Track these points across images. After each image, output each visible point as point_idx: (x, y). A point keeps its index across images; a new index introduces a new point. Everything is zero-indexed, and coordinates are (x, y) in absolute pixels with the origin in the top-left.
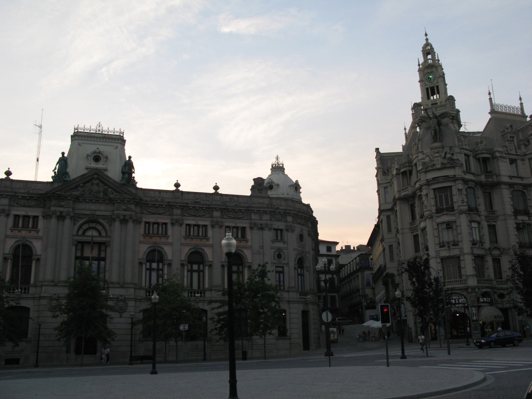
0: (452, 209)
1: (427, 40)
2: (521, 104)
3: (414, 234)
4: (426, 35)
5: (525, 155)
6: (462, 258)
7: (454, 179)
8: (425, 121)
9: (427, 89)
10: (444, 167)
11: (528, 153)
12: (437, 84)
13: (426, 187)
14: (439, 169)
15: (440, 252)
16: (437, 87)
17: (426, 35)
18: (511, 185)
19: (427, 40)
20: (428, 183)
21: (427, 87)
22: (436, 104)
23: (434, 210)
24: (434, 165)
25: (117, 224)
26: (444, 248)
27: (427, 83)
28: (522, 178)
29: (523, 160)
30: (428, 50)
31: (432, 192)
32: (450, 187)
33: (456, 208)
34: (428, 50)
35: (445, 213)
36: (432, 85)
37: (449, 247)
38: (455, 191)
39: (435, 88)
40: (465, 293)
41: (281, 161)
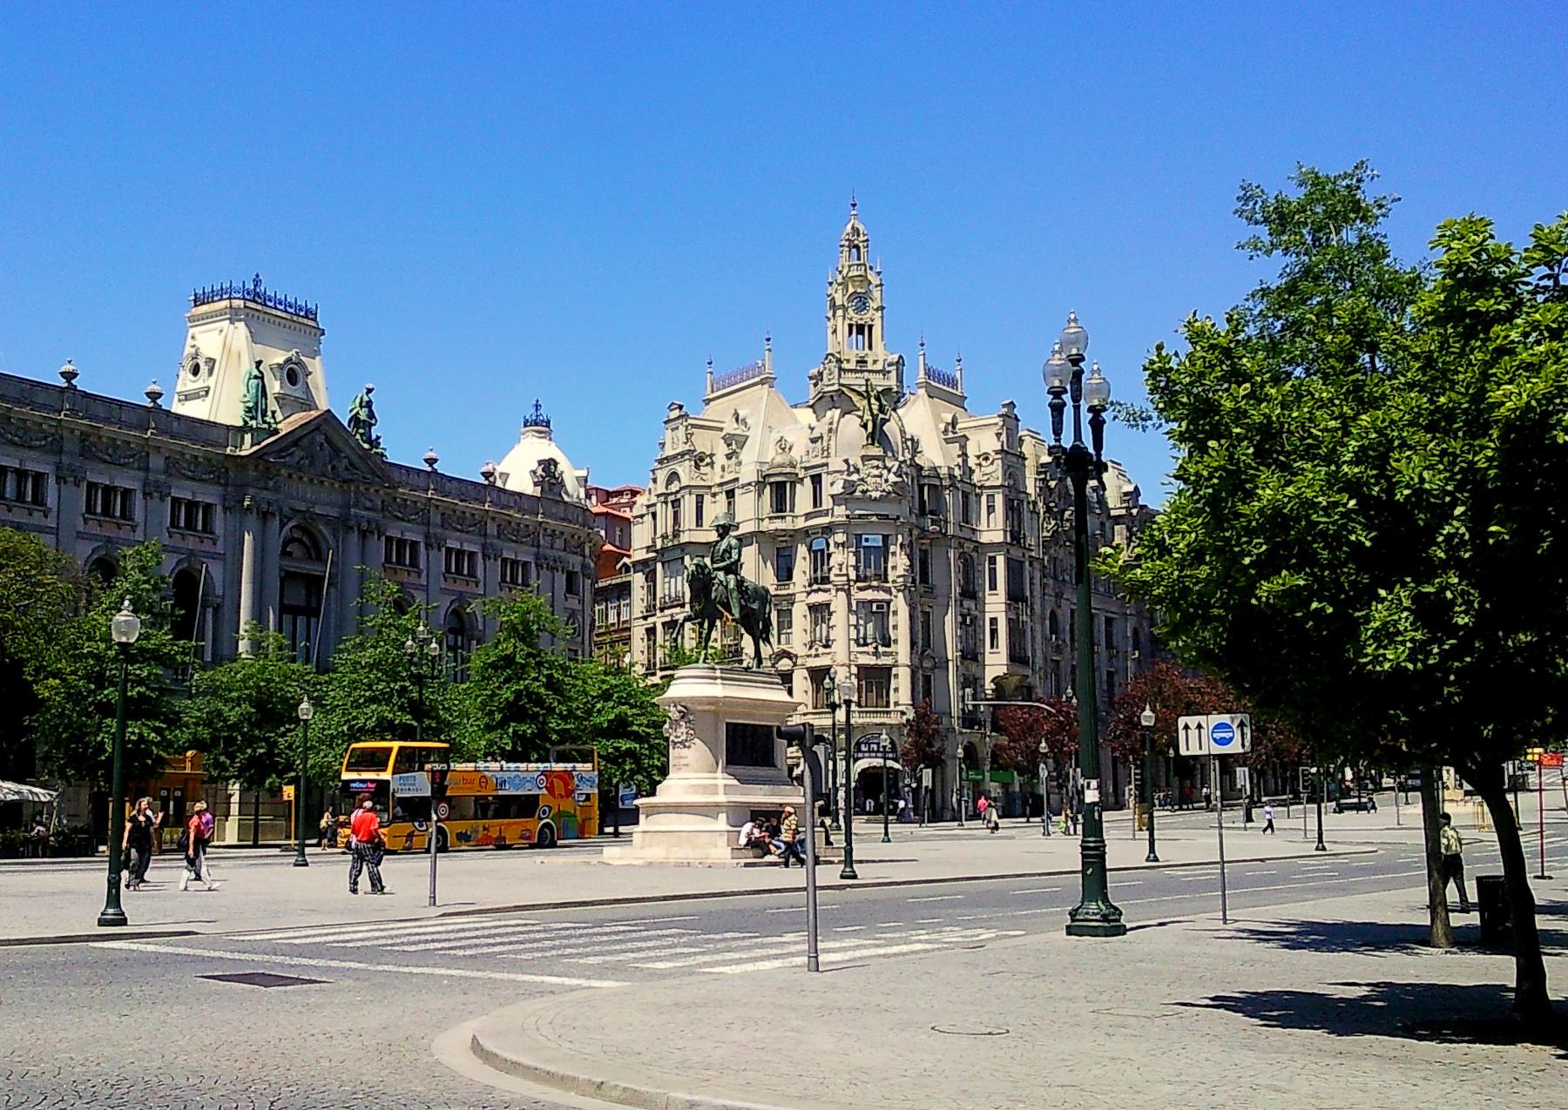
9: (850, 326)
11: (987, 484)
16: (870, 327)
23: (853, 576)
25: (354, 537)
41: (544, 413)
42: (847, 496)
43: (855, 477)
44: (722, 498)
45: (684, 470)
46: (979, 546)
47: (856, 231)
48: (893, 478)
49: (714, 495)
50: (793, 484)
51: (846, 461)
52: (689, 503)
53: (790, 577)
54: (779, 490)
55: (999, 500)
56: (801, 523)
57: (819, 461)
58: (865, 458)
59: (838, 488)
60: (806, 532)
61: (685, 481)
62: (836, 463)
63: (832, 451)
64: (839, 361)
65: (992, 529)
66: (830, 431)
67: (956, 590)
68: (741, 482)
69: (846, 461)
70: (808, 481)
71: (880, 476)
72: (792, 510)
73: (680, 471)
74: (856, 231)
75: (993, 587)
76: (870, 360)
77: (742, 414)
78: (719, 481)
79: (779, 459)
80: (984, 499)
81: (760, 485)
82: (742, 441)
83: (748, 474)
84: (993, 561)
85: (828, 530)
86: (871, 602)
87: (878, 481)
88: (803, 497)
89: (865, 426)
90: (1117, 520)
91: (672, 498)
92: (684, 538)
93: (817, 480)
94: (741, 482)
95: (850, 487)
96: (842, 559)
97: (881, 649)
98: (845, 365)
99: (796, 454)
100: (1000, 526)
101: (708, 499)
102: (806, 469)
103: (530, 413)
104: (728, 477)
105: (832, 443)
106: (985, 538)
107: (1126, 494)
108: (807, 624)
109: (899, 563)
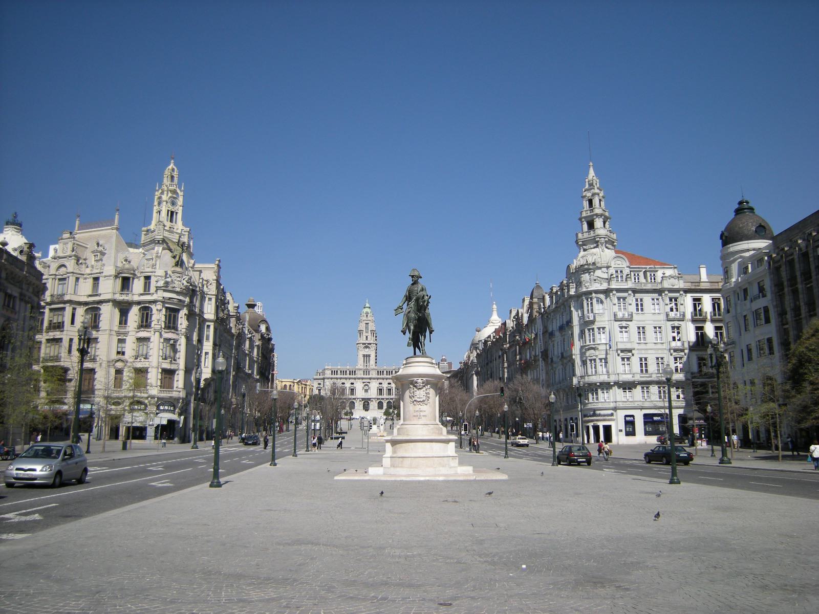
3: (120, 337)
9: (168, 211)
11: (209, 293)
15: (163, 363)
16: (177, 213)
20: (164, 301)
21: (169, 209)
23: (163, 326)
26: (166, 361)
35: (173, 331)
36: (174, 210)
39: (175, 213)
41: (19, 219)
42: (166, 287)
43: (169, 280)
44: (91, 281)
45: (71, 265)
46: (205, 320)
47: (173, 170)
48: (186, 284)
49: (85, 279)
50: (133, 279)
51: (166, 272)
52: (72, 280)
53: (126, 323)
54: (126, 283)
55: (214, 300)
56: (136, 298)
58: (173, 272)
59: (161, 283)
60: (139, 303)
61: (70, 269)
62: (160, 272)
63: (157, 266)
64: (164, 226)
65: (209, 311)
68: (103, 274)
69: (166, 272)
70: (142, 279)
72: (132, 291)
73: (67, 264)
74: (173, 170)
76: (175, 227)
77: (101, 243)
78: (88, 271)
79: (127, 266)
80: (207, 299)
81: (116, 277)
82: (103, 254)
83: (110, 270)
84: (208, 326)
85: (155, 302)
86: (170, 339)
87: (179, 283)
88: (138, 285)
90: (233, 316)
91: (60, 277)
92: (67, 298)
93: (148, 278)
94: (103, 274)
95: (167, 283)
96: (158, 316)
97: (173, 362)
98: (166, 228)
99: (134, 264)
100: (213, 311)
101: (81, 280)
102: (142, 272)
103: (11, 218)
104: (95, 271)
106: (206, 316)
107: (235, 307)
108: (134, 346)
109: (183, 322)
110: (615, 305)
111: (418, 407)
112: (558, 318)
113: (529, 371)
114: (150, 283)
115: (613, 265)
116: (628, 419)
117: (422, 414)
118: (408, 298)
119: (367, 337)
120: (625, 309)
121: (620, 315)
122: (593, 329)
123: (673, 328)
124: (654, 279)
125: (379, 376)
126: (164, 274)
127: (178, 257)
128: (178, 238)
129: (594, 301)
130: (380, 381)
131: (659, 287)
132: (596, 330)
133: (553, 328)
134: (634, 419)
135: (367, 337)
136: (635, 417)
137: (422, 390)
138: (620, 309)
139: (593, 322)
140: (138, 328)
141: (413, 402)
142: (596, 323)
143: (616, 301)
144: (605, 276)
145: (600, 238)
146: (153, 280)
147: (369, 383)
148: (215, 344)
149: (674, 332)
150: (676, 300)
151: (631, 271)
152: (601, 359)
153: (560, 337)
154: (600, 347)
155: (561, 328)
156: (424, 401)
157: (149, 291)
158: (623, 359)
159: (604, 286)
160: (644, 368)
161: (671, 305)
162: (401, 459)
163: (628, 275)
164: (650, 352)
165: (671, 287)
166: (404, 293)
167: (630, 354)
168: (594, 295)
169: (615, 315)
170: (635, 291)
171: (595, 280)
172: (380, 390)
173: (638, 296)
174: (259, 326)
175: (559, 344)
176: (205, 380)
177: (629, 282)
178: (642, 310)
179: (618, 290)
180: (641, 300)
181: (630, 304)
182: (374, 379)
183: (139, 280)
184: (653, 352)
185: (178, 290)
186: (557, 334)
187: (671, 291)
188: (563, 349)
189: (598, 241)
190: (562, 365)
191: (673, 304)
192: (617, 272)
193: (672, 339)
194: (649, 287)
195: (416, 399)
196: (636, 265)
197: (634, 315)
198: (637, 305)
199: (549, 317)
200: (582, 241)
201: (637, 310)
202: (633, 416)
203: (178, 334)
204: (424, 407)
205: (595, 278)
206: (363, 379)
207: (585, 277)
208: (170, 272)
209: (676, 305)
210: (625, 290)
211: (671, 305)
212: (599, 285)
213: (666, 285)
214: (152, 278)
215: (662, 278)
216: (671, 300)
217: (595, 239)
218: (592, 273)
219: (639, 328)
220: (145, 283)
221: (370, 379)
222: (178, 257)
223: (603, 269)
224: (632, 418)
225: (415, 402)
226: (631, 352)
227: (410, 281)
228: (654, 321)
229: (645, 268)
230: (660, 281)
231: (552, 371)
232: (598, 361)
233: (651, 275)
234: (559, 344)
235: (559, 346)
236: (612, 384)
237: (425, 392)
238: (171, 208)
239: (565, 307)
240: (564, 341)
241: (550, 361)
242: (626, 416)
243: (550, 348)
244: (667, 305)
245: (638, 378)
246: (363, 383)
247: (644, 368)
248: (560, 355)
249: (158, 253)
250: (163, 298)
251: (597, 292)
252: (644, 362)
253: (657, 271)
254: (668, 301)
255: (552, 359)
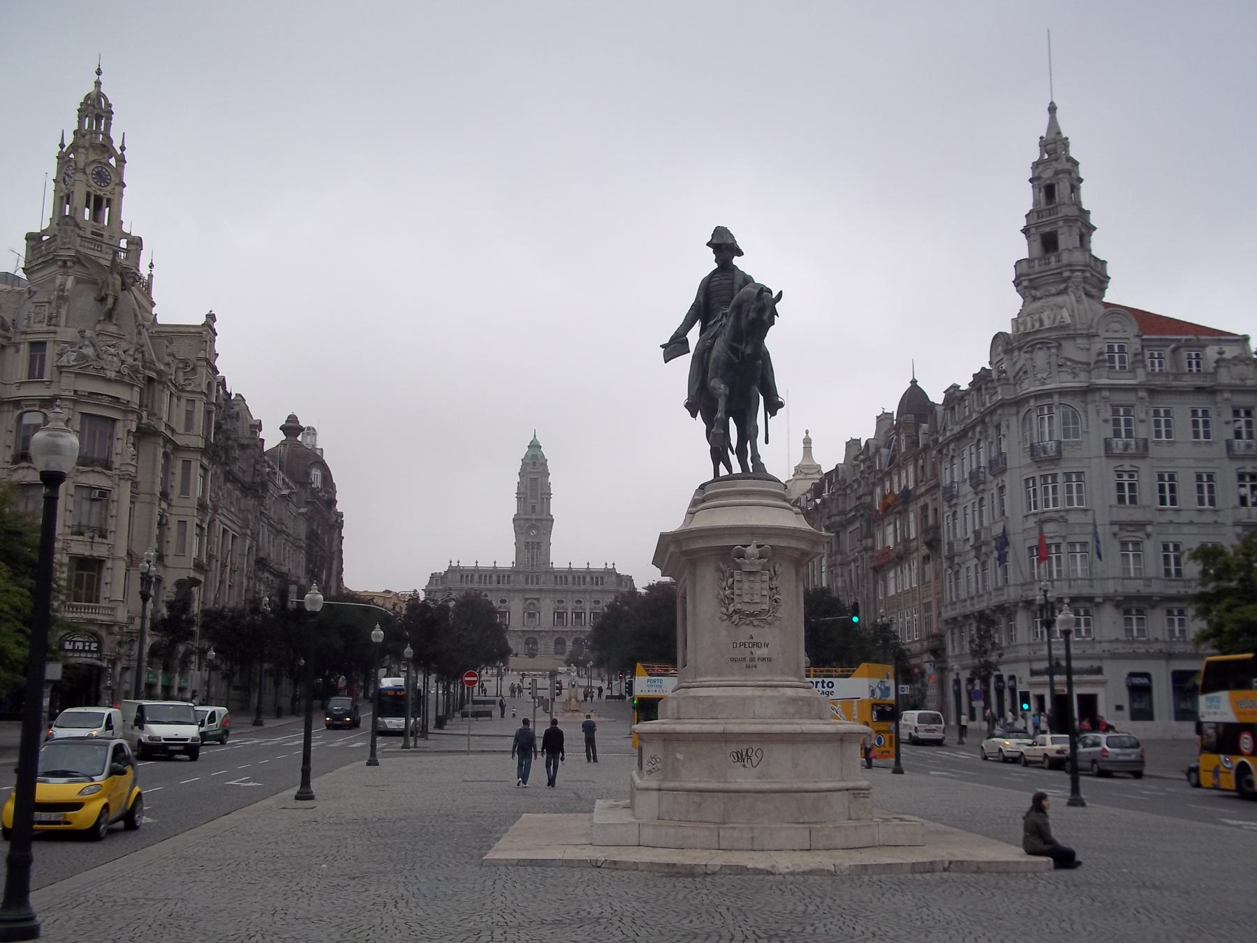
0: (107, 465)
1: (98, 84)
2: (151, 276)
4: (99, 72)
5: (183, 390)
6: (109, 564)
7: (126, 409)
8: (83, 265)
9: (88, 194)
10: (119, 381)
11: (188, 388)
12: (109, 196)
13: (69, 404)
14: (109, 380)
15: (72, 544)
17: (99, 72)
18: (168, 440)
19: (98, 84)
20: (77, 398)
22: (102, 235)
24: (102, 368)
26: (81, 538)
27: (92, 182)
28: (173, 431)
29: (179, 399)
30: (96, 109)
31: (78, 417)
32: (114, 421)
33: (117, 465)
34: (96, 109)
37: (92, 538)
38: (120, 431)
40: (103, 633)
43: (89, 351)
46: (177, 448)
51: (82, 332)
57: (44, 327)
59: (70, 358)
60: (16, 403)
63: (62, 321)
66: (60, 298)
67: (158, 489)
69: (82, 332)
70: (25, 349)
71: (117, 355)
75: (185, 490)
84: (187, 463)
86: (92, 488)
89: (102, 300)
93: (38, 347)
97: (97, 539)
102: (25, 333)
105: (63, 312)
106: (180, 441)
110: (1106, 421)
111: (744, 633)
112: (966, 454)
113: (892, 574)
114: (43, 358)
115: (1103, 334)
116: (1137, 681)
117: (759, 652)
118: (703, 310)
119: (534, 507)
120: (1129, 434)
121: (1118, 445)
122: (1054, 476)
123: (1241, 477)
124: (1198, 365)
125: (558, 587)
126: (77, 338)
127: (110, 301)
128: (110, 257)
129: (1058, 414)
130: (559, 596)
131: (1207, 383)
132: (1060, 479)
133: (952, 478)
134: (1150, 680)
135: (534, 507)
136: (1154, 678)
137: (758, 578)
138: (1117, 434)
139: (1056, 459)
140: (15, 462)
141: (730, 616)
142: (1063, 464)
143: (1108, 415)
144: (1081, 357)
145: (1073, 271)
146: (51, 351)
147: (537, 599)
148: (202, 507)
149: (1243, 486)
150: (1248, 413)
151: (1143, 347)
152: (1072, 544)
153: (970, 496)
154: (1072, 518)
155: (976, 480)
156: (762, 612)
157: (41, 375)
158: (1124, 544)
159: (1080, 382)
160: (1173, 567)
161: (1237, 425)
162: (696, 798)
163: (1136, 355)
164: (1186, 529)
165: (1238, 382)
166: (688, 297)
167: (1141, 534)
168: (1056, 398)
169: (1108, 445)
170: (1152, 392)
171: (1060, 366)
172: (560, 615)
173: (1162, 403)
174: (308, 474)
175: (969, 511)
176: (179, 584)
177: (1140, 372)
178: (1169, 434)
179: (1113, 389)
180: (1167, 413)
181: (1142, 421)
182: (549, 591)
183: (18, 351)
184: (1194, 529)
185: (112, 375)
186: (967, 488)
187: (1235, 390)
188: (977, 522)
189: (1069, 278)
190: (977, 557)
191: (1242, 422)
192: (1111, 348)
193: (1237, 502)
194: (1187, 382)
195: (739, 606)
196: (1154, 334)
197: (1151, 445)
198: (1157, 424)
199: (945, 451)
200: (1030, 280)
201: (1158, 434)
202: (1147, 675)
203: (109, 477)
204: (759, 634)
205: (1061, 361)
206: (524, 591)
207: (1041, 357)
208: (88, 333)
209: (1249, 424)
210: (1133, 389)
211: (1237, 425)
212: (1070, 378)
213: (1224, 377)
214: (49, 345)
215: (1217, 361)
216: (1236, 413)
217: (1061, 273)
218: (1053, 351)
219: (1161, 477)
220: (32, 360)
221: (540, 591)
222: (110, 301)
223: (1079, 341)
224: (1145, 681)
225: (735, 617)
226: (1144, 529)
227: (709, 263)
228: (1196, 460)
229: (1173, 340)
230: (1211, 370)
231: (950, 571)
232: (1063, 548)
233: (1189, 357)
234: (969, 511)
235: (969, 517)
236: (1099, 600)
237: (766, 585)
238: (95, 189)
239: (985, 430)
240: (981, 506)
241: (945, 550)
242: (1132, 675)
243: (946, 523)
244: (1227, 423)
245: (1156, 588)
246: (527, 599)
247: (1173, 567)
248: (970, 535)
249: (63, 290)
250: (75, 392)
251: (1063, 393)
252: (1171, 552)
253: (1205, 346)
254: (1229, 416)
255: (950, 545)
